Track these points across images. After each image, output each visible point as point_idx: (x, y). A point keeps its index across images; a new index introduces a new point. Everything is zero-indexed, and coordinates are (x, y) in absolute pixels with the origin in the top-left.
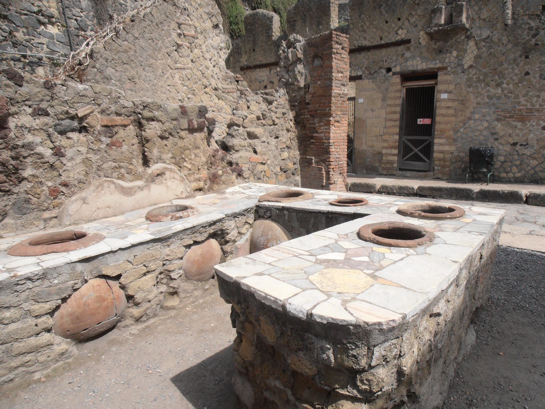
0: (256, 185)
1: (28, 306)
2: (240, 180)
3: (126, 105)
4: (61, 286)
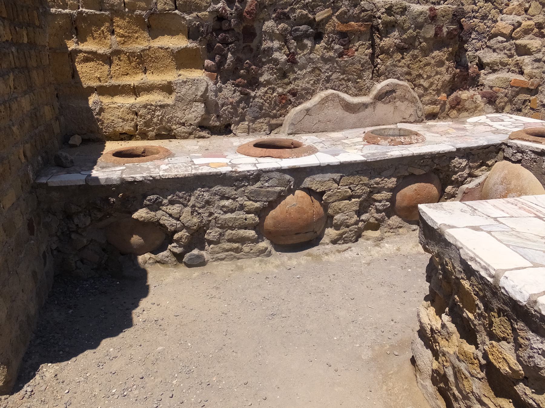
0: (511, 118)
1: (242, 200)
2: (490, 108)
3: (366, 7)
4: (269, 189)
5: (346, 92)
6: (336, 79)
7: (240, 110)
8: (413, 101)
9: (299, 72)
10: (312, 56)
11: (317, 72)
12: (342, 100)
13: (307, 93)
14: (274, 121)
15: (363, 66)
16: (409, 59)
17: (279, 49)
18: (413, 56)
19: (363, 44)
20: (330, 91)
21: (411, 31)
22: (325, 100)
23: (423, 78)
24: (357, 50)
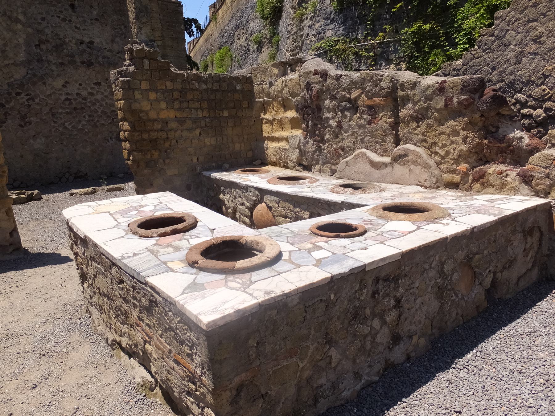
2: (525, 188)
3: (384, 86)
5: (375, 152)
6: (368, 141)
7: (315, 157)
8: (426, 166)
9: (345, 134)
10: (350, 123)
11: (356, 135)
12: (368, 158)
13: (350, 150)
14: (333, 167)
15: (385, 132)
16: (424, 127)
17: (333, 118)
18: (428, 124)
19: (385, 115)
20: (364, 150)
21: (421, 103)
22: (357, 156)
23: (439, 146)
24: (381, 119)
